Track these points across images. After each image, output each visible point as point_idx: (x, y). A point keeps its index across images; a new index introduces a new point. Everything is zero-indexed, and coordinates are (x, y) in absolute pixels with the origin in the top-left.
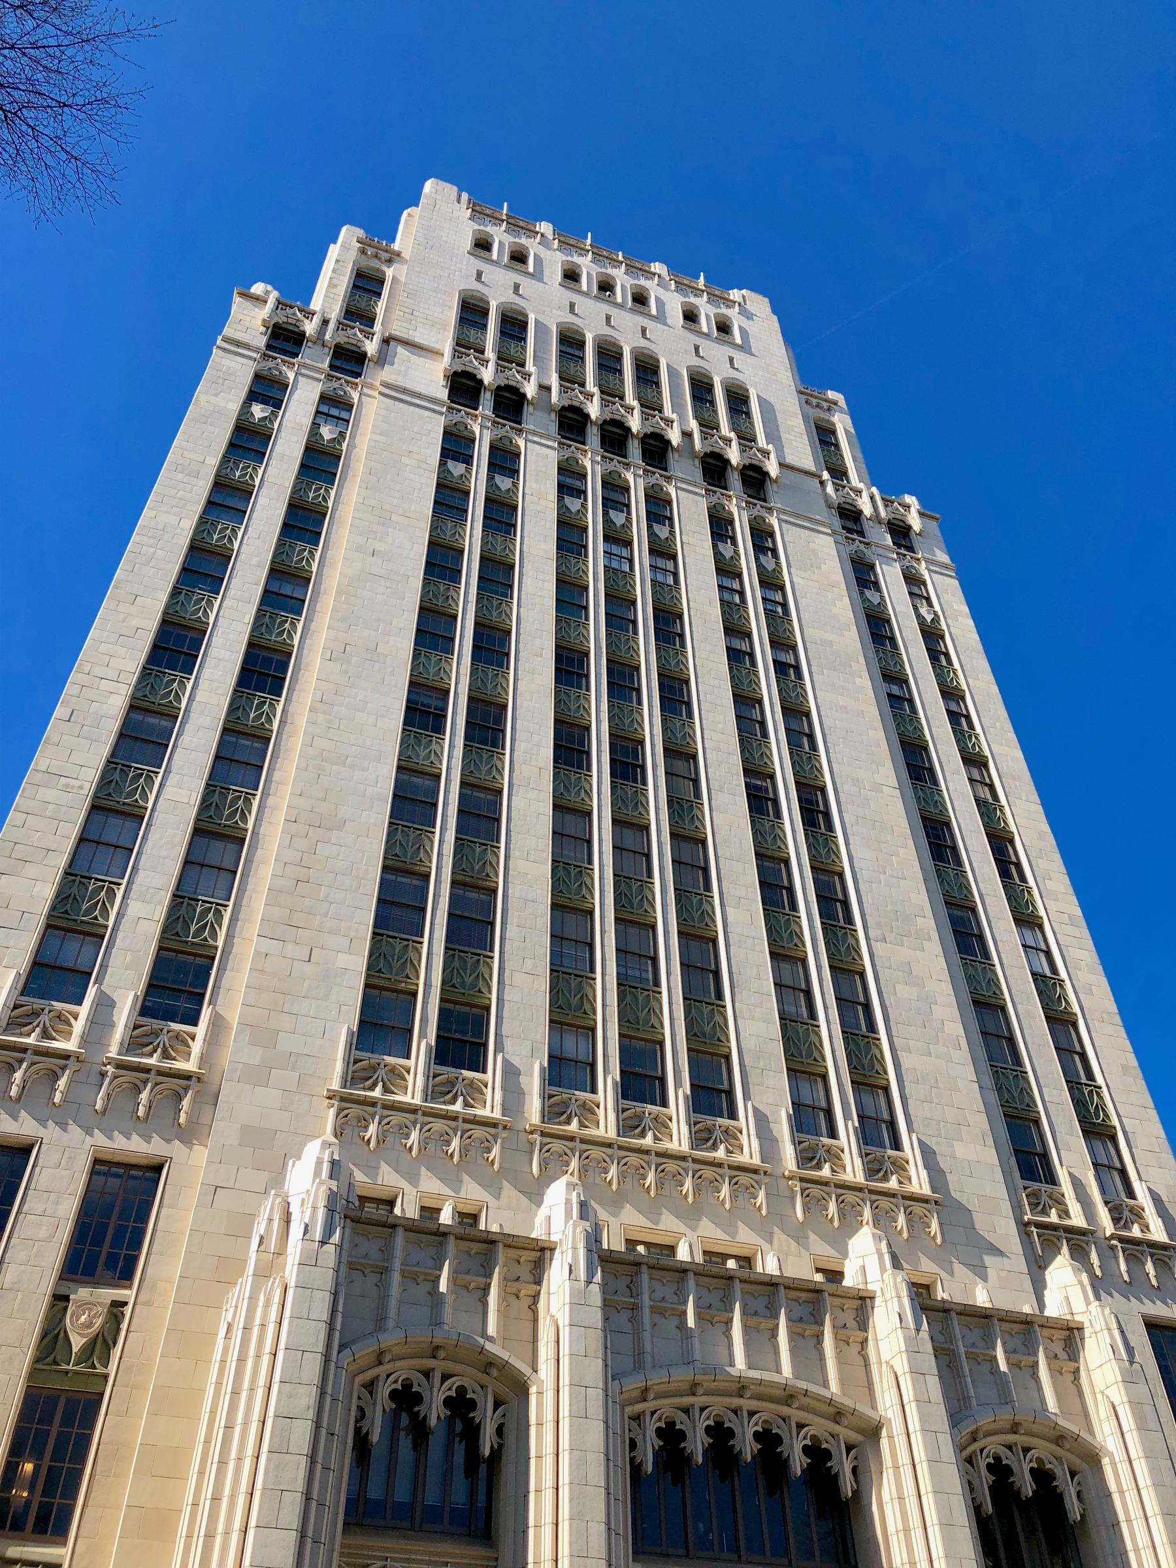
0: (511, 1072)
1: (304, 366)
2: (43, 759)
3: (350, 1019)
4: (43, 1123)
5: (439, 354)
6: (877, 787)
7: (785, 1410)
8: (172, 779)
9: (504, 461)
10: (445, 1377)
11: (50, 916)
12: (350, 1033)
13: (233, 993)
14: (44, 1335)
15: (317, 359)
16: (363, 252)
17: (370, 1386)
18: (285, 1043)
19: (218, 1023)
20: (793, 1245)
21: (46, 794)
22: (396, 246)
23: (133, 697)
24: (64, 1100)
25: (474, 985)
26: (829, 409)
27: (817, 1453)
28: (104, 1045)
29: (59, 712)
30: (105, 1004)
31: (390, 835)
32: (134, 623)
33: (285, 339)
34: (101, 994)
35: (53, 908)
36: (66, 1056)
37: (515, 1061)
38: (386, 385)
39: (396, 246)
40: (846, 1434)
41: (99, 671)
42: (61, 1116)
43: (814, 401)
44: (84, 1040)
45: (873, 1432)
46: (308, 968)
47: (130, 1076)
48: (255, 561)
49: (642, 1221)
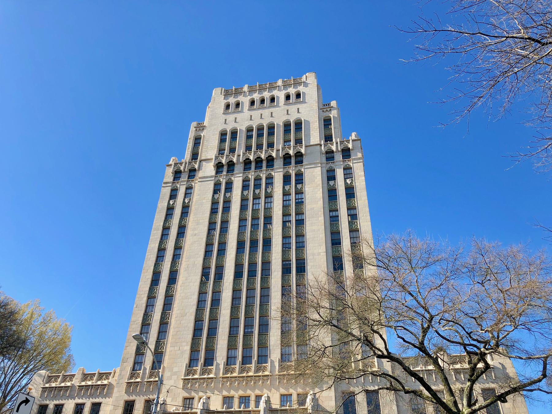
0: (218, 365)
1: (182, 182)
2: (133, 319)
5: (212, 159)
6: (319, 254)
8: (155, 314)
9: (229, 186)
11: (136, 353)
12: (187, 364)
13: (167, 360)
16: (196, 130)
18: (175, 369)
19: (164, 367)
21: (134, 326)
23: (148, 296)
25: (212, 345)
28: (145, 378)
29: (135, 306)
30: (145, 369)
32: (147, 277)
33: (177, 174)
34: (144, 367)
36: (138, 382)
37: (218, 362)
38: (200, 178)
41: (141, 293)
42: (138, 394)
43: (325, 110)
46: (179, 352)
47: (149, 383)
49: (243, 393)
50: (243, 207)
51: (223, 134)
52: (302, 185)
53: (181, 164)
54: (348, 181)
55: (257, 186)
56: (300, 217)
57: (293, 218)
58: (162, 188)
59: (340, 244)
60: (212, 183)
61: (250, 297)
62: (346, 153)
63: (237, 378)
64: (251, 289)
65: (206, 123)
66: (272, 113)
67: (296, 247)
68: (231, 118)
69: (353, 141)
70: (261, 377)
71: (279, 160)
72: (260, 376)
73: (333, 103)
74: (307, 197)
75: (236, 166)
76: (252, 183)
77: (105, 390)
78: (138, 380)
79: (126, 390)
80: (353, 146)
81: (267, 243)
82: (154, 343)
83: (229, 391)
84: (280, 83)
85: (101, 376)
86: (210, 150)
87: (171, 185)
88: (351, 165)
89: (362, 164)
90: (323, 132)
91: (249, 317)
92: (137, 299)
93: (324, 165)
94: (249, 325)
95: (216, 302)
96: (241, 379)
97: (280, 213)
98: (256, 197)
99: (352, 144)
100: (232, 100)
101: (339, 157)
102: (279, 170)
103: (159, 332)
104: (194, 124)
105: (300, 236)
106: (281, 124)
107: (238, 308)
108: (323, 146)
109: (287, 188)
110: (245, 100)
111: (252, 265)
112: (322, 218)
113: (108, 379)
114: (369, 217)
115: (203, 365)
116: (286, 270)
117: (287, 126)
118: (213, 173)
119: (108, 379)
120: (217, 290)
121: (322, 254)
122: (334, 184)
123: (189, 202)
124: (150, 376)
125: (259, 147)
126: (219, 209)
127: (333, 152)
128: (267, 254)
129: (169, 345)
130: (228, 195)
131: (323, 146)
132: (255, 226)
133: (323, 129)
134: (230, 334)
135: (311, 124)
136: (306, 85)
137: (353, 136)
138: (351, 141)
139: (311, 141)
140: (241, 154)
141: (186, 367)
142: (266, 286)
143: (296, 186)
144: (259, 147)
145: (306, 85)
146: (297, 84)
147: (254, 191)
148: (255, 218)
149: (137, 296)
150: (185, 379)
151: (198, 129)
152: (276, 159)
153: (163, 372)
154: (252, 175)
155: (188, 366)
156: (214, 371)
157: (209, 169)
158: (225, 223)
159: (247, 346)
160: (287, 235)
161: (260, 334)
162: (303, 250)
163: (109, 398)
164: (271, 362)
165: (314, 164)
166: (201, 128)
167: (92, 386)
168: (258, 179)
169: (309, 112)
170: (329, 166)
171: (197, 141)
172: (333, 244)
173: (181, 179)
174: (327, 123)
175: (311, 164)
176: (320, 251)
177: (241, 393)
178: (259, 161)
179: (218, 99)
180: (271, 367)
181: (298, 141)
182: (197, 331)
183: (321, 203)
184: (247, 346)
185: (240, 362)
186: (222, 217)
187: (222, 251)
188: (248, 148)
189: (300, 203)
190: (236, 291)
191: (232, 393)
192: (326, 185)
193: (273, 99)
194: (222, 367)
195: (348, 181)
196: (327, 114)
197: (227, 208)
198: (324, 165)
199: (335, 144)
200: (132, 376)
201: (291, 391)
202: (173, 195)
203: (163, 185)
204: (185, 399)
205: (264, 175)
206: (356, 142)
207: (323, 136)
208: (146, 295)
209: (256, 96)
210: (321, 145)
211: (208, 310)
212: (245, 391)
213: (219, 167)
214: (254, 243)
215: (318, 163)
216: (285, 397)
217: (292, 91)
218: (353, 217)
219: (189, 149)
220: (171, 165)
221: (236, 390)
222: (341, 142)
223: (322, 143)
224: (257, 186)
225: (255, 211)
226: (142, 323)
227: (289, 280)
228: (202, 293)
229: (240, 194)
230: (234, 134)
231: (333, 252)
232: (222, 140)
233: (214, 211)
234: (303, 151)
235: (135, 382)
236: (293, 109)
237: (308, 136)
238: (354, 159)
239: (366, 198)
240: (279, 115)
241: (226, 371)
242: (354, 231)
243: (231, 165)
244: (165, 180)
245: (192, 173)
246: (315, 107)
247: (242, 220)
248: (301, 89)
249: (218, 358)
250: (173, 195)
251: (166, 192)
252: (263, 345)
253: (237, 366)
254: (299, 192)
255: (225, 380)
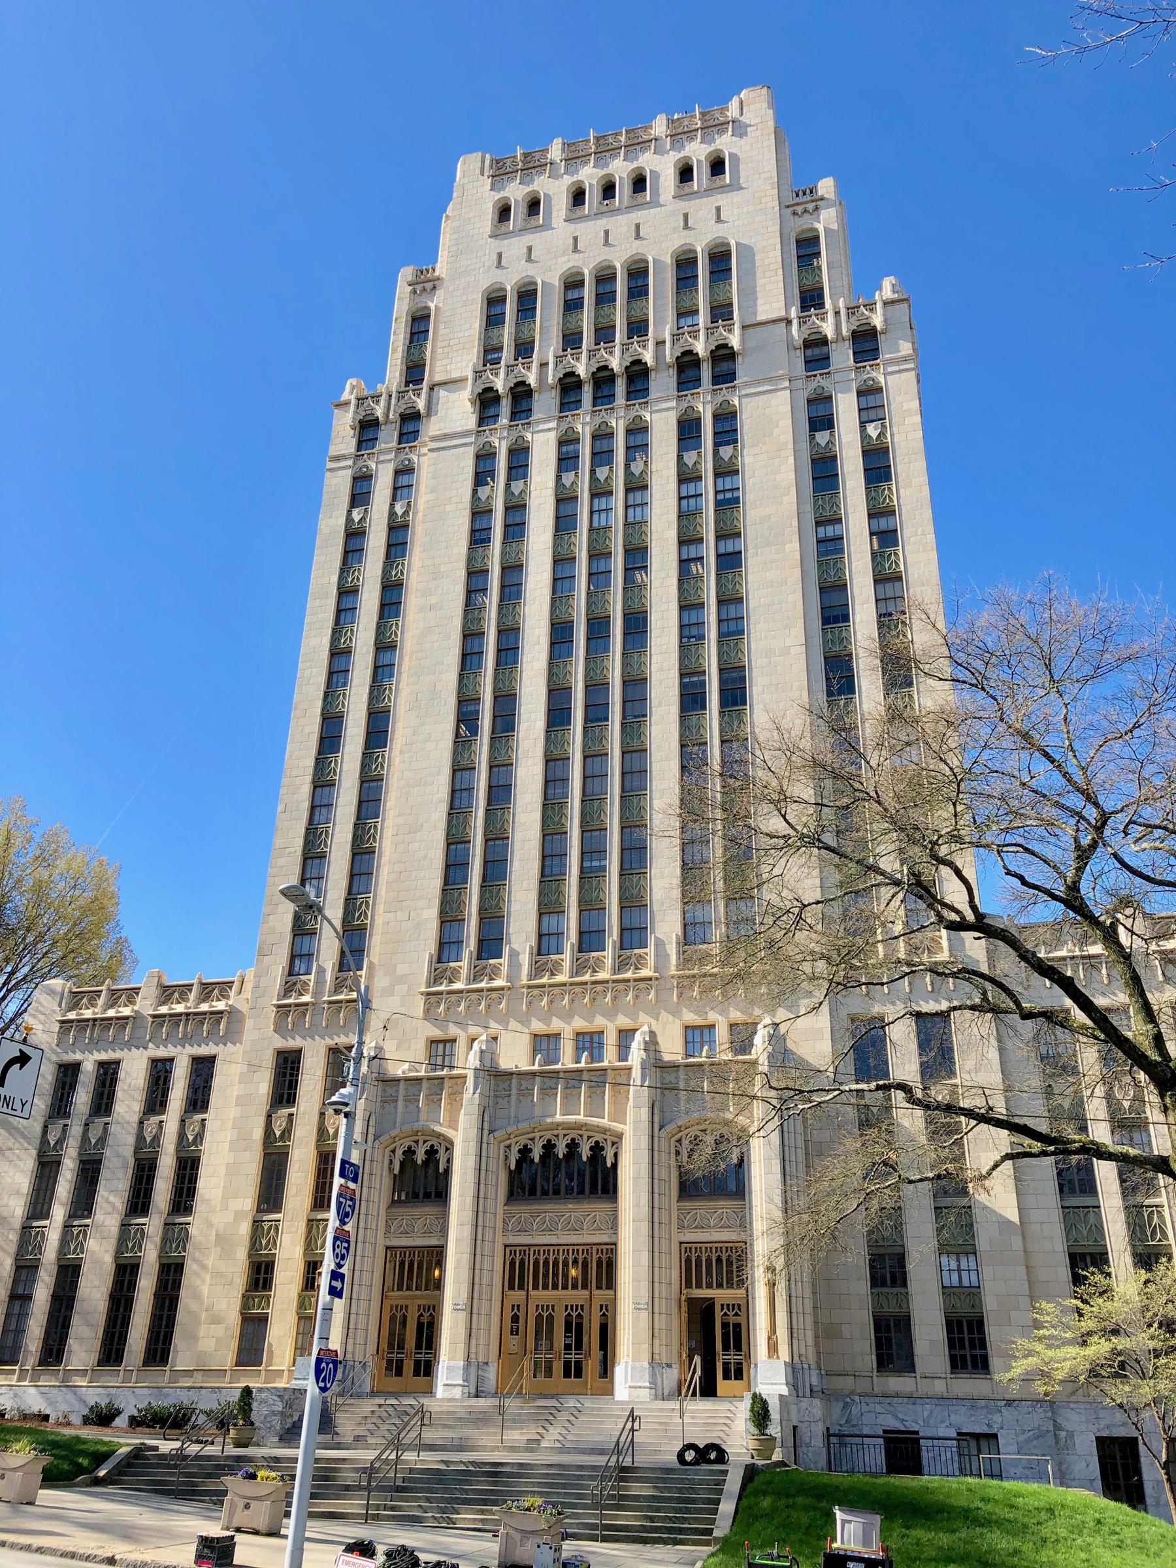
0: (514, 954)
1: (381, 452)
2: (278, 842)
3: (431, 946)
4: (304, 1038)
6: (786, 651)
7: (580, 1132)
8: (337, 828)
10: (425, 1142)
12: (431, 956)
13: (377, 947)
14: (319, 1129)
15: (388, 438)
16: (415, 292)
17: (393, 1151)
18: (402, 969)
19: (371, 966)
20: (671, 1017)
21: (281, 861)
22: (437, 274)
23: (314, 782)
24: (311, 1025)
26: (817, 208)
27: (597, 1148)
29: (280, 808)
30: (321, 971)
31: (449, 822)
32: (307, 730)
33: (367, 429)
34: (318, 965)
35: (294, 926)
36: (306, 1004)
37: (515, 946)
38: (434, 439)
39: (437, 274)
40: (610, 1139)
41: (294, 774)
42: (310, 1034)
43: (799, 209)
44: (316, 994)
45: (620, 1136)
46: (409, 924)
48: (365, 649)
50: (564, 524)
51: (494, 301)
52: (735, 448)
53: (376, 398)
54: (873, 430)
55: (602, 456)
56: (729, 546)
57: (709, 550)
58: (328, 474)
59: (846, 618)
60: (470, 452)
61: (593, 777)
62: (866, 343)
63: (568, 988)
64: (594, 756)
65: (441, 269)
66: (638, 226)
67: (721, 635)
68: (514, 248)
69: (886, 304)
70: (632, 984)
71: (665, 374)
72: (628, 981)
73: (826, 187)
74: (749, 483)
75: (536, 396)
76: (585, 450)
77: (223, 1024)
78: (306, 998)
79: (276, 1024)
80: (885, 321)
81: (637, 625)
82: (342, 902)
83: (546, 1020)
84: (659, 127)
85: (207, 990)
86: (456, 353)
87: (350, 462)
88: (882, 379)
89: (913, 374)
90: (796, 278)
91: (592, 828)
92: (283, 791)
93: (799, 384)
94: (592, 851)
95: (501, 793)
96: (578, 989)
97: (672, 535)
98: (600, 491)
99: (884, 315)
100: (516, 192)
101: (842, 356)
102: (664, 405)
103: (352, 876)
104: (406, 273)
105: (730, 600)
106: (668, 260)
107: (562, 805)
108: (795, 322)
109: (690, 458)
110: (554, 189)
111: (596, 688)
112: (793, 547)
113: (227, 997)
114: (931, 538)
115: (475, 955)
116: (691, 699)
117: (685, 265)
118: (471, 422)
119: (227, 997)
120: (502, 759)
121: (793, 650)
122: (831, 442)
123: (406, 513)
124: (337, 989)
125: (604, 334)
126: (493, 529)
127: (824, 341)
128: (636, 656)
129: (380, 908)
130: (517, 487)
131: (795, 322)
132: (598, 577)
133: (795, 271)
134: (543, 875)
135: (758, 257)
136: (740, 129)
137: (887, 289)
138: (879, 306)
139: (760, 309)
140: (551, 360)
141: (431, 962)
142: (635, 744)
143: (716, 452)
144: (604, 334)
145: (740, 129)
146: (713, 127)
147: (593, 472)
148: (598, 554)
149: (285, 781)
150: (428, 994)
151: (419, 288)
152: (656, 369)
153: (370, 976)
154: (584, 424)
155: (435, 959)
156: (504, 970)
157: (456, 412)
158: (513, 571)
159: (590, 905)
160: (693, 600)
161: (624, 872)
162: (738, 642)
163: (234, 1044)
164: (656, 945)
165: (770, 380)
166: (429, 286)
167: (188, 1014)
168: (602, 436)
169: (750, 218)
170: (814, 385)
171: (419, 324)
172: (826, 621)
173: (381, 445)
174: (806, 249)
175: (760, 382)
176: (789, 642)
177: (579, 1024)
178: (603, 379)
179: (473, 190)
180: (656, 955)
181: (721, 312)
182: (454, 869)
183: (790, 500)
184: (590, 905)
185: (573, 945)
186: (503, 554)
187: (509, 652)
188: (571, 340)
189: (728, 504)
190: (554, 762)
191: (556, 1024)
192: (805, 445)
193: (639, 183)
194: (525, 960)
195: (873, 430)
196: (804, 223)
197: (515, 529)
198: (799, 384)
199: (830, 316)
200: (288, 989)
201: (713, 1017)
202: (360, 496)
203: (330, 465)
204: (433, 1042)
205: (621, 422)
206: (896, 307)
207: (797, 291)
208: (309, 779)
209: (589, 175)
210: (789, 322)
211: (481, 813)
212: (589, 1018)
213: (487, 401)
214: (598, 628)
215: (780, 378)
216: (697, 1032)
217: (698, 152)
218: (885, 537)
219: (395, 351)
220: (347, 403)
221: (567, 1017)
222: (852, 310)
223: (794, 313)
224: (602, 456)
225: (598, 533)
226: (304, 853)
227: (700, 727)
228: (461, 768)
229: (551, 483)
230: (527, 297)
231: (825, 642)
232: (493, 320)
233: (479, 538)
234: (735, 341)
235: (297, 1005)
236: (701, 209)
237: (750, 293)
238: (890, 362)
239: (924, 479)
240: (659, 232)
241: (538, 970)
242: (887, 579)
243: (522, 395)
244: (333, 450)
245: (410, 423)
246: (771, 202)
247: (562, 560)
248: (725, 143)
249: (513, 938)
250: (360, 496)
251: (339, 483)
252: (634, 903)
253: (567, 957)
254: (726, 470)
255: (536, 992)
